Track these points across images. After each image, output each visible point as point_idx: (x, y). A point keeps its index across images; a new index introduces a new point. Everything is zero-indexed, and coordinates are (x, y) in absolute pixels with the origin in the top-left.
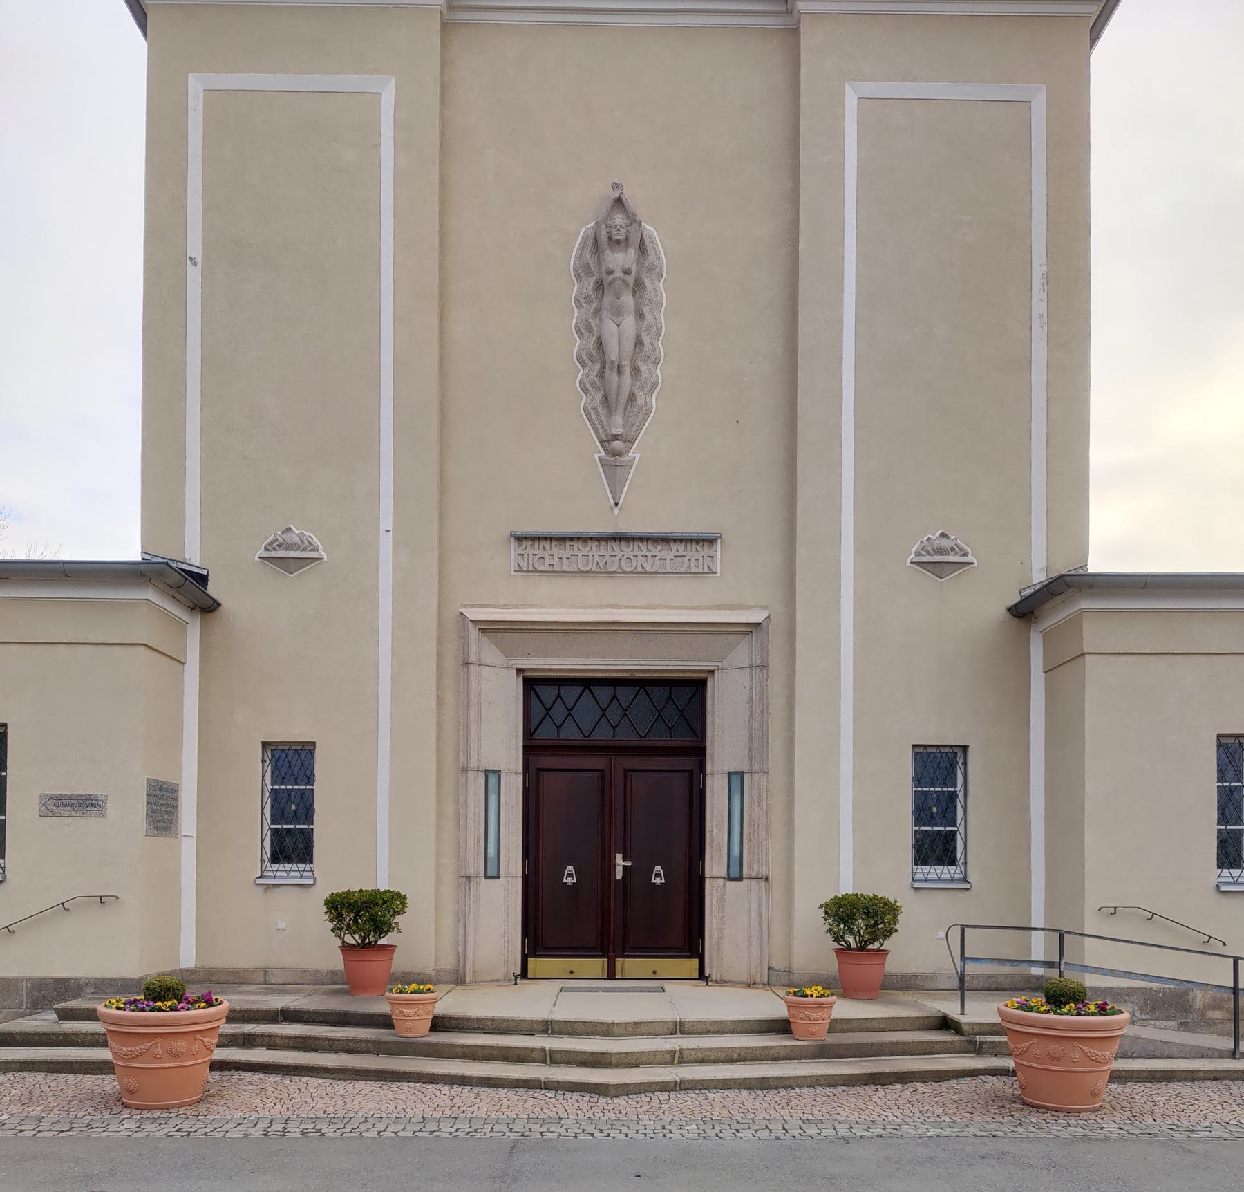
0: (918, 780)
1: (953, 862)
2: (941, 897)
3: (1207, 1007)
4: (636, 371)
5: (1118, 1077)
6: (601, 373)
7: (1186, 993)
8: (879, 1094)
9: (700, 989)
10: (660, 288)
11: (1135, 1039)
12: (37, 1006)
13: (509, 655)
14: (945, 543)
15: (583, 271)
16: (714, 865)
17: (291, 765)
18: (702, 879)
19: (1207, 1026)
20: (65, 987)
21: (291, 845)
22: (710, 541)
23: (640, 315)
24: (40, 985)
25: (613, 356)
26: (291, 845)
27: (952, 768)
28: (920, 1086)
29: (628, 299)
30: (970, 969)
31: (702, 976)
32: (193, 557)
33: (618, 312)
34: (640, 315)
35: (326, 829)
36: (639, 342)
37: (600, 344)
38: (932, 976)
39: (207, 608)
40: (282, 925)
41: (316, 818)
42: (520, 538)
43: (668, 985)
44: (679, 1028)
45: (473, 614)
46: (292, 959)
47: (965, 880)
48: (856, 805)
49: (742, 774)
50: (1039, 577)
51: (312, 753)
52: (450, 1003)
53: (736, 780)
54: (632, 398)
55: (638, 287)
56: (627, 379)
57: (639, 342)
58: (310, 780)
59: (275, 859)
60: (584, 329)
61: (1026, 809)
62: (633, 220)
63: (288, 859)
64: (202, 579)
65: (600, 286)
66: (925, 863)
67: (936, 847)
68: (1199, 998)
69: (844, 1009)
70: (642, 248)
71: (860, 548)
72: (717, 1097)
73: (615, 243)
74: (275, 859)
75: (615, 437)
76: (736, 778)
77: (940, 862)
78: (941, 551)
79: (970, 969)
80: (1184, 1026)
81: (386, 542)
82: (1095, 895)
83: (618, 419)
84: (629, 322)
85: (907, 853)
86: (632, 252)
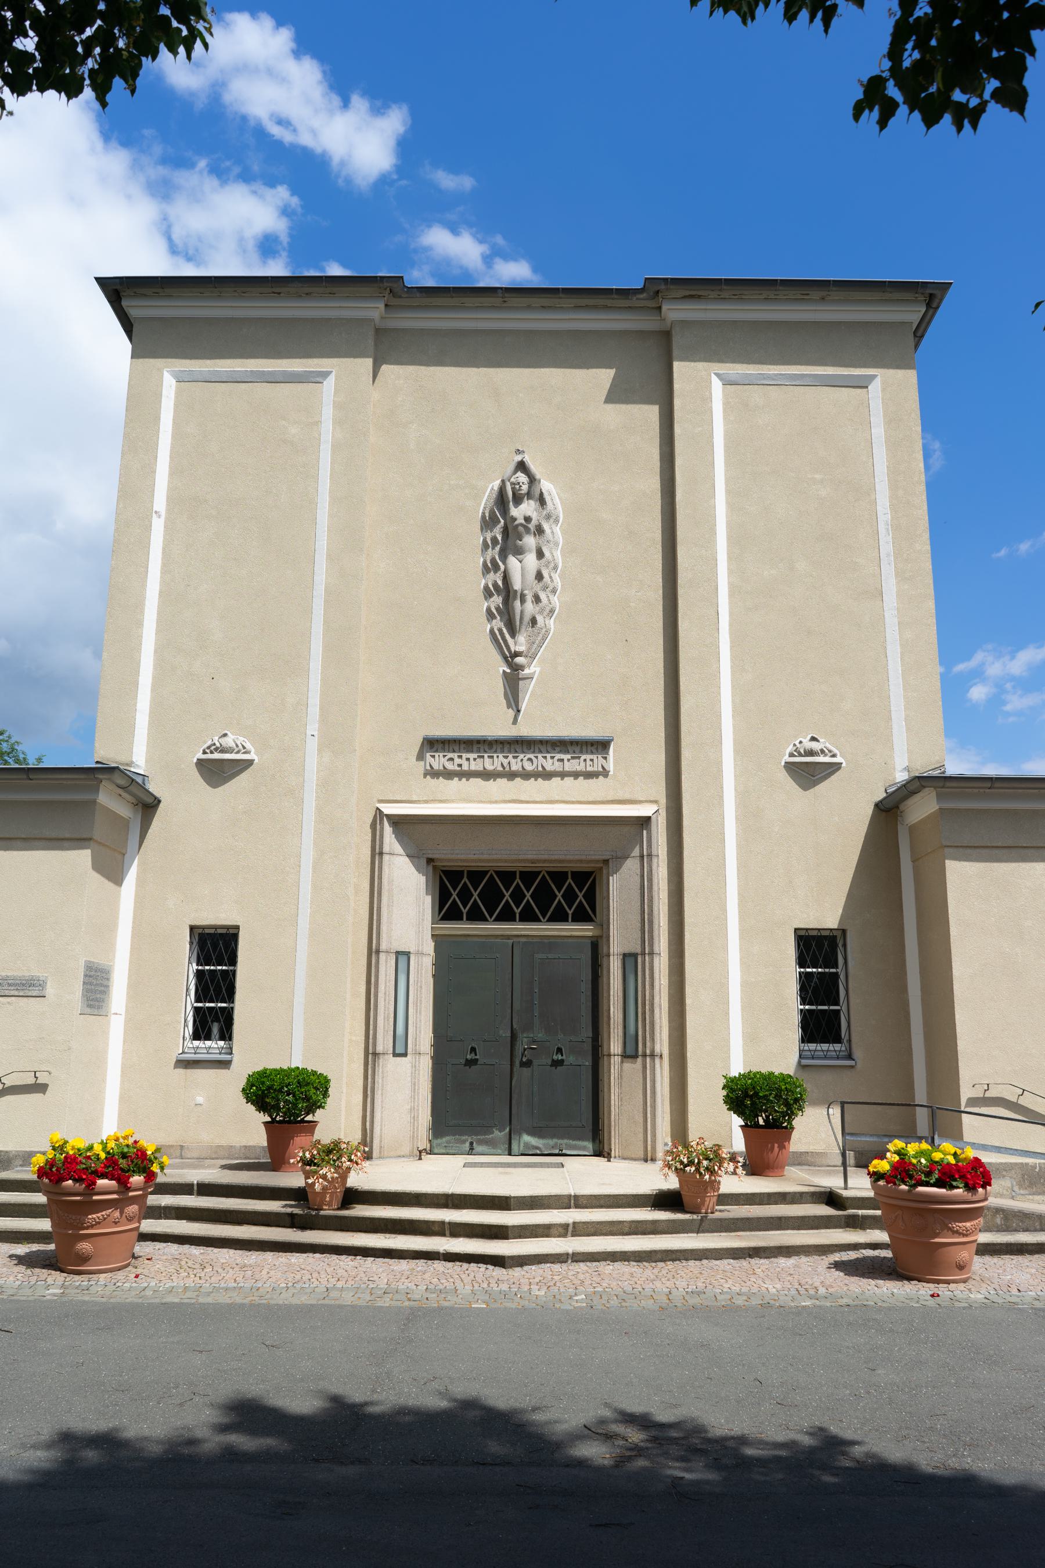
1: (838, 1040)
4: (537, 599)
10: (554, 531)
14: (815, 746)
23: (540, 554)
31: (601, 1152)
34: (540, 554)
36: (539, 576)
37: (506, 578)
40: (200, 1099)
45: (389, 809)
47: (850, 1057)
48: (745, 985)
49: (634, 956)
50: (901, 777)
53: (630, 962)
54: (534, 621)
55: (540, 531)
57: (539, 576)
58: (233, 961)
61: (903, 989)
62: (532, 480)
67: (820, 1026)
70: (542, 501)
71: (740, 751)
73: (518, 500)
75: (517, 654)
76: (630, 960)
78: (811, 753)
83: (521, 638)
84: (531, 559)
85: (795, 1033)
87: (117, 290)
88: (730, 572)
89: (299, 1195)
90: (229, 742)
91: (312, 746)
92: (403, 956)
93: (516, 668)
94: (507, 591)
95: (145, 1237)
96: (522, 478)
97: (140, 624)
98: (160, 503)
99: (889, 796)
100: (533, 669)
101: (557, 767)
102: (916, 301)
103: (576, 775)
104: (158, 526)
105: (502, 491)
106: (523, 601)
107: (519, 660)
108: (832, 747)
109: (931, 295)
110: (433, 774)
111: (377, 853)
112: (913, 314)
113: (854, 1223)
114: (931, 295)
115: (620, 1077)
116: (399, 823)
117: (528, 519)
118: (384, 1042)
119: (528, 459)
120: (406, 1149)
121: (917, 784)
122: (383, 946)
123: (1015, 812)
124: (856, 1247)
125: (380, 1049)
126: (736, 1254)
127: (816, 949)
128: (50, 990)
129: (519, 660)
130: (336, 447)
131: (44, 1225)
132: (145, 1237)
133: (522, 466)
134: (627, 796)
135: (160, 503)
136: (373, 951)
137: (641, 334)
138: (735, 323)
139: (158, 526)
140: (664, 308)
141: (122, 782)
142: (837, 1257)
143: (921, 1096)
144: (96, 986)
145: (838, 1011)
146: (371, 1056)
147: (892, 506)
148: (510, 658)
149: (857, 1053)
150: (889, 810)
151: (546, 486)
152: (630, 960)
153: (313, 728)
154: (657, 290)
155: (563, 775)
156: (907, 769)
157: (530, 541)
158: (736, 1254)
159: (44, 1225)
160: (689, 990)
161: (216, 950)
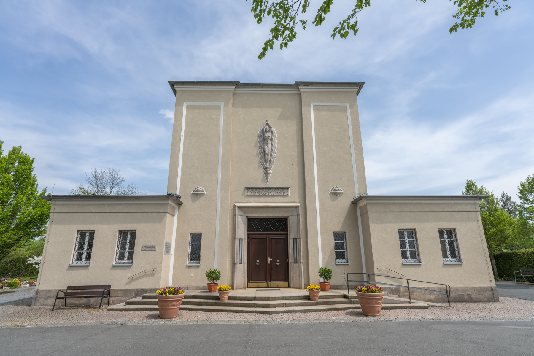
0: (335, 240)
1: (344, 258)
2: (342, 267)
3: (404, 292)
4: (271, 155)
5: (383, 308)
6: (264, 155)
7: (399, 289)
8: (331, 313)
9: (289, 289)
10: (275, 139)
11: (388, 299)
12: (136, 296)
13: (244, 213)
14: (337, 189)
15: (260, 136)
16: (291, 260)
17: (196, 238)
18: (288, 263)
19: (404, 296)
20: (143, 291)
21: (195, 256)
22: (288, 189)
23: (272, 144)
24: (137, 290)
25: (267, 152)
26: (195, 256)
27: (343, 236)
28: (340, 311)
29: (269, 141)
30: (350, 283)
31: (289, 287)
32: (178, 193)
33: (267, 144)
34: (272, 144)
35: (203, 252)
36: (272, 150)
37: (264, 150)
38: (342, 286)
39: (180, 204)
40: (192, 275)
41: (201, 250)
42: (247, 189)
43: (281, 289)
44: (285, 298)
45: (237, 204)
46: (194, 284)
47: (347, 262)
48: (322, 245)
49: (296, 239)
50: (357, 196)
51: (201, 235)
52: (232, 293)
53: (295, 240)
54: (271, 160)
55: (272, 139)
56: (269, 156)
57: (272, 150)
58: (200, 241)
59: (191, 260)
60: (260, 147)
61: (359, 246)
62: (270, 127)
63: (194, 260)
64: (180, 198)
65: (264, 139)
66: (338, 258)
67: (340, 255)
68: (402, 289)
69: (321, 294)
70: (272, 132)
71: (319, 190)
72: (294, 314)
73: (266, 131)
74: (191, 260)
75: (267, 168)
76: (295, 240)
77: (342, 258)
78: (336, 190)
79: (350, 283)
80: (399, 297)
81: (219, 189)
82: (376, 266)
83: (268, 164)
84: (270, 146)
85: (334, 257)
86: (270, 133)
87: (172, 84)
88: (316, 148)
89: (217, 298)
90: (199, 189)
91: (219, 189)
92: (241, 239)
93: (267, 171)
94: (263, 153)
95: (181, 309)
96: (268, 127)
97: (178, 161)
98: (183, 133)
99: (355, 200)
100: (271, 171)
101: (276, 194)
102: (357, 86)
103: (281, 196)
104: (182, 138)
105: (263, 130)
106: (268, 155)
107: (268, 169)
108: (341, 189)
109: (360, 85)
110: (248, 196)
111: (235, 215)
112: (356, 89)
113: (352, 303)
114: (360, 85)
115: (292, 267)
116: (240, 208)
117: (269, 136)
118: (236, 261)
119: (269, 123)
120: (242, 287)
121: (361, 198)
122: (236, 237)
123: (384, 204)
124: (352, 308)
125: (236, 262)
126: (324, 310)
127: (339, 237)
128: (157, 249)
129: (268, 169)
130: (224, 120)
131: (157, 307)
132: (181, 309)
133: (267, 124)
134: (293, 201)
135: (183, 133)
136: (234, 239)
137: (294, 94)
138: (316, 91)
139: (182, 138)
140: (300, 87)
141: (175, 198)
142: (348, 311)
143: (365, 271)
144: (168, 247)
145: (344, 252)
146: (233, 264)
147: (353, 133)
148: (265, 169)
149: (349, 261)
150: (355, 203)
151: (273, 129)
152: (295, 240)
153: (219, 185)
154: (298, 85)
155: (278, 196)
156: (359, 194)
157: (269, 141)
158: (324, 310)
159: (157, 307)
160: (309, 247)
161: (196, 238)
